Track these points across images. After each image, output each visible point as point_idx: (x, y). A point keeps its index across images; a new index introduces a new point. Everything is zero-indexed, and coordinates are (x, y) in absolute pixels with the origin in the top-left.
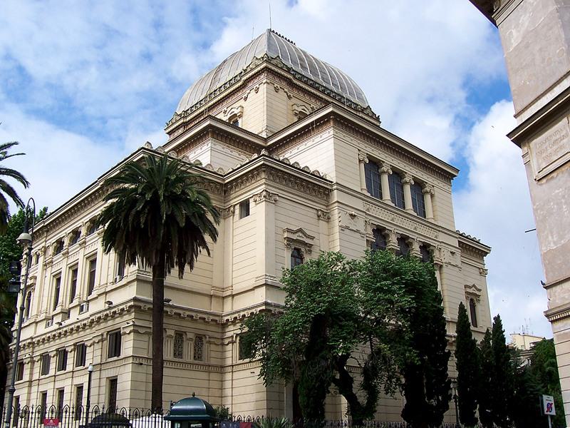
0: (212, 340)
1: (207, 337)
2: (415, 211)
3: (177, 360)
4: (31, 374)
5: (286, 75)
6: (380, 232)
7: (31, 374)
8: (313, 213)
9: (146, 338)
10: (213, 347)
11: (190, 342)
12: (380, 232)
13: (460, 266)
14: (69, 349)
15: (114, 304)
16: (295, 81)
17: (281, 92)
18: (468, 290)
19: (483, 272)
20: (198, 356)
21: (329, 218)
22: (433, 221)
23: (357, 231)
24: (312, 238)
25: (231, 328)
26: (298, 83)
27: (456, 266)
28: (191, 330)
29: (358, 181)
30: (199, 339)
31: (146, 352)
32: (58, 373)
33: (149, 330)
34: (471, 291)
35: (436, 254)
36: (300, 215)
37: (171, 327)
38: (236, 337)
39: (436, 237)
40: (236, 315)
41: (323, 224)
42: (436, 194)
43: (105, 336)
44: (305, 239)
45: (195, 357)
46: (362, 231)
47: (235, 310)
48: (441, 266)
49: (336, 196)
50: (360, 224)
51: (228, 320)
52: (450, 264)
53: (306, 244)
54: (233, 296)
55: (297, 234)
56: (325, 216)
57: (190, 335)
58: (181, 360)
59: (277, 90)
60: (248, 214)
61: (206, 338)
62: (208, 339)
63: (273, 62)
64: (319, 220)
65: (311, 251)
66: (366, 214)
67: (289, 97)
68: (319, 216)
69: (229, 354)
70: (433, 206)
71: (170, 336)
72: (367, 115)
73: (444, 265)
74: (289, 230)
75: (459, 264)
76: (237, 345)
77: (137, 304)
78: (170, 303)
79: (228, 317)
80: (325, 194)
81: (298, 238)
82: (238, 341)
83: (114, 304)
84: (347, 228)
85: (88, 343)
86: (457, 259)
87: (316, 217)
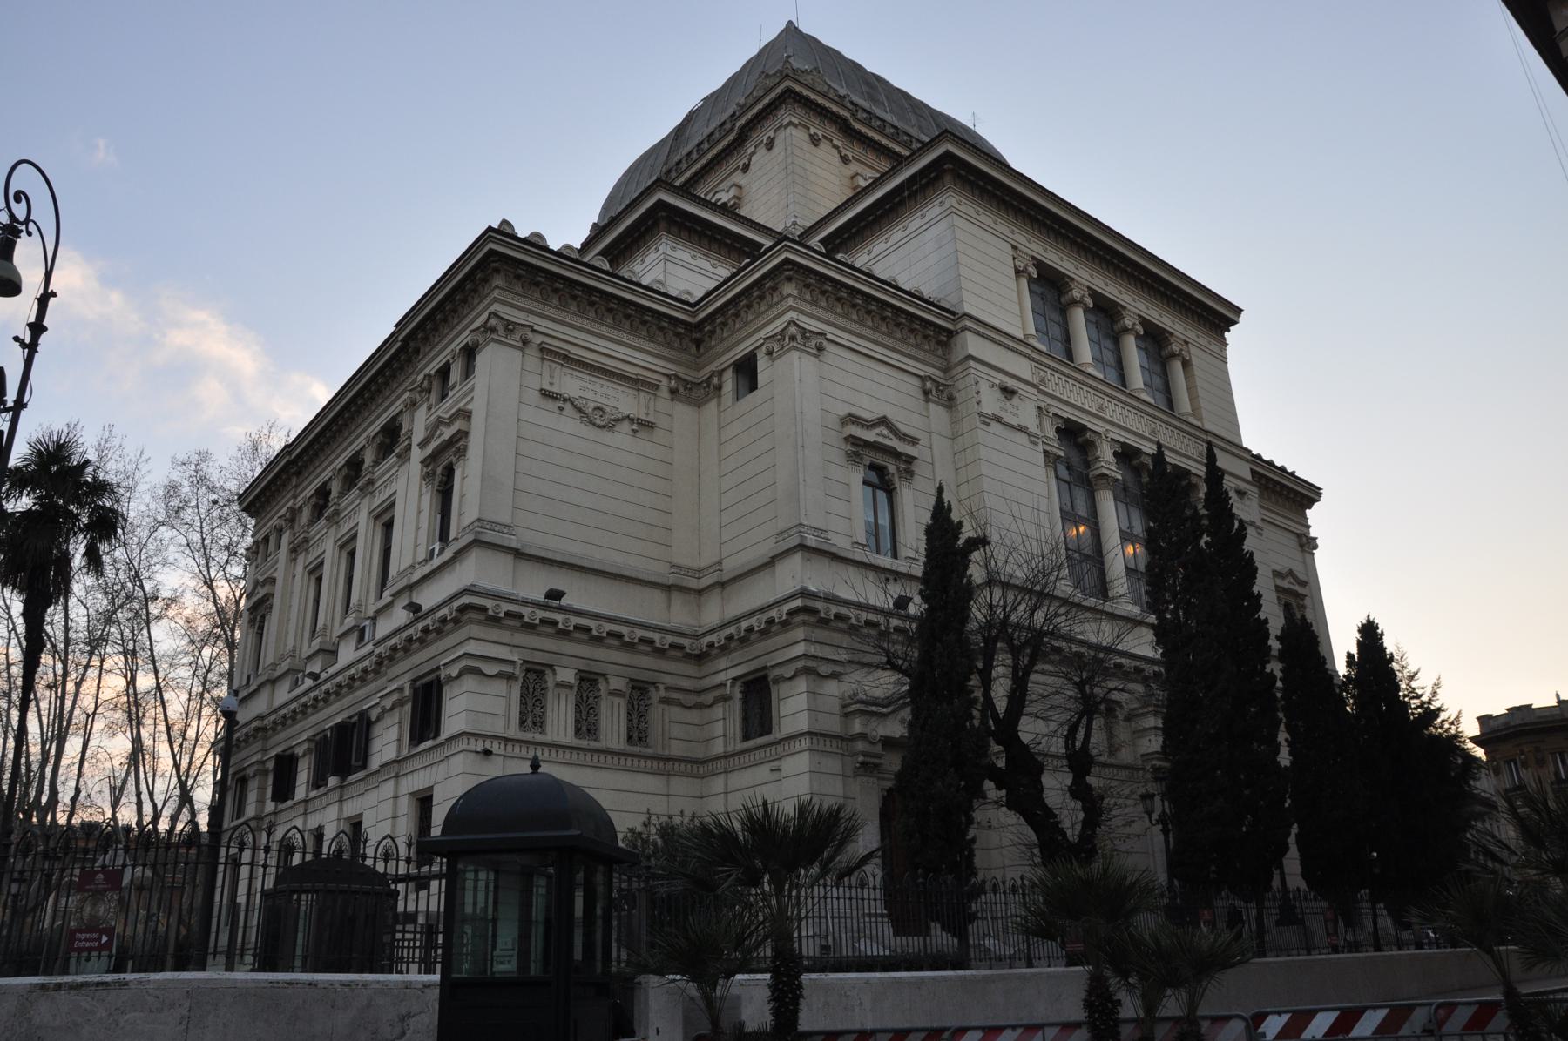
0: (674, 695)
1: (661, 687)
3: (584, 743)
6: (1072, 433)
9: (500, 687)
10: (675, 712)
11: (617, 700)
13: (1259, 523)
15: (425, 608)
18: (1279, 582)
20: (637, 734)
21: (951, 398)
22: (1192, 420)
25: (722, 663)
28: (617, 666)
30: (639, 689)
31: (501, 722)
33: (508, 669)
34: (1285, 584)
37: (565, 660)
38: (733, 685)
40: (731, 630)
46: (1033, 428)
49: (973, 345)
50: (1025, 412)
51: (711, 645)
54: (722, 585)
55: (877, 431)
57: (617, 683)
58: (593, 745)
60: (753, 386)
61: (657, 689)
62: (662, 693)
64: (927, 401)
66: (1040, 391)
68: (926, 393)
71: (562, 685)
76: (737, 705)
78: (564, 602)
79: (713, 638)
80: (939, 343)
81: (880, 440)
82: (738, 695)
83: (425, 608)
87: (921, 397)
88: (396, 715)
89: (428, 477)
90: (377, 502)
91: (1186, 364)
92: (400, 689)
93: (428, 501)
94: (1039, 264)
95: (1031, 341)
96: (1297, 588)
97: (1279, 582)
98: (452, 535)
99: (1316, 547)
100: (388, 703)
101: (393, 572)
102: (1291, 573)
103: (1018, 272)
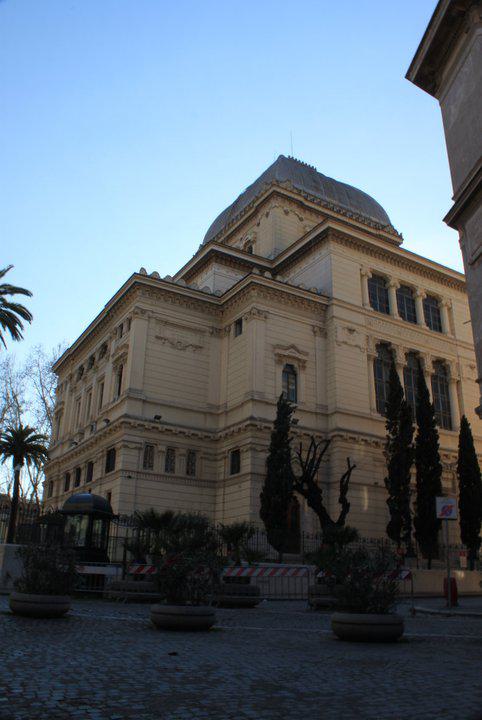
4: (58, 491)
5: (296, 197)
7: (58, 491)
12: (385, 347)
14: (82, 467)
16: (307, 203)
17: (291, 214)
21: (326, 333)
24: (307, 354)
26: (311, 205)
41: (319, 339)
44: (297, 355)
47: (229, 424)
53: (299, 360)
56: (323, 332)
59: (286, 213)
60: (241, 333)
63: (283, 185)
65: (304, 367)
67: (301, 220)
68: (315, 332)
72: (388, 233)
77: (126, 420)
84: (346, 343)
85: (94, 460)
89: (114, 369)
93: (115, 378)
101: (103, 404)
103: (362, 276)
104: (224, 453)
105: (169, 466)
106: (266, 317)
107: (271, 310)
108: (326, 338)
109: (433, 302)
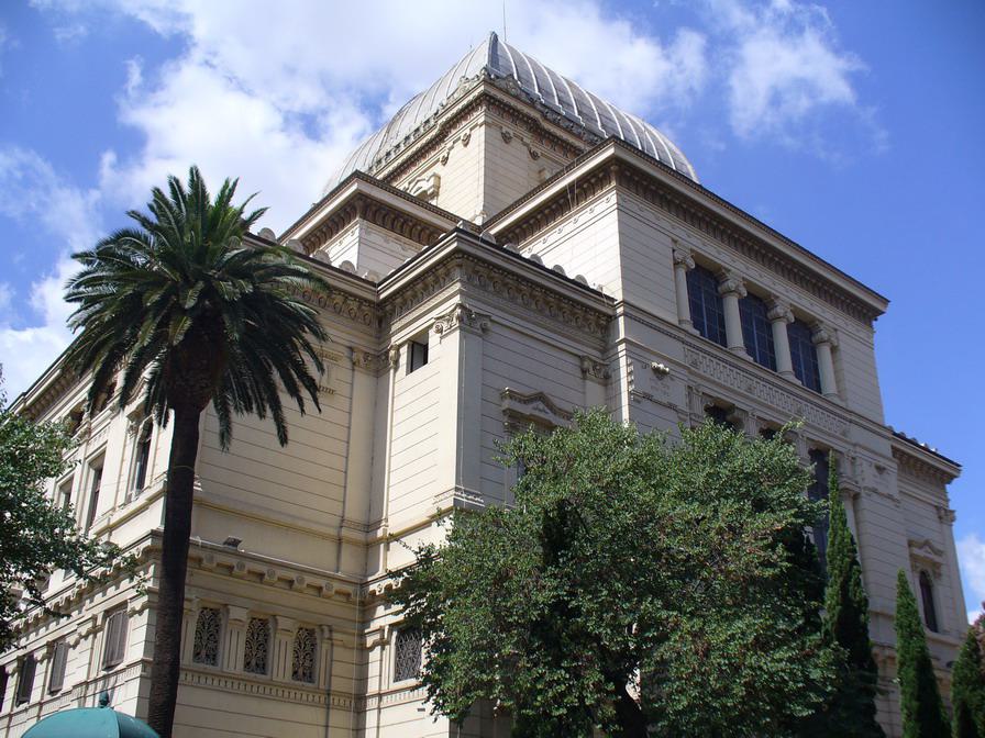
2: (798, 376)
8: (571, 365)
13: (897, 496)
14: (38, 656)
18: (916, 551)
19: (945, 516)
21: (607, 377)
22: (836, 400)
23: (671, 406)
27: (890, 497)
29: (672, 304)
32: (16, 710)
34: (921, 553)
35: (846, 468)
36: (545, 365)
39: (844, 434)
42: (842, 346)
43: (99, 622)
45: (295, 673)
48: (856, 497)
50: (677, 393)
52: (875, 491)
55: (535, 404)
64: (584, 378)
66: (691, 373)
68: (584, 372)
69: (373, 670)
70: (836, 372)
73: (863, 493)
74: (512, 395)
75: (894, 492)
81: (537, 413)
84: (648, 397)
86: (892, 483)
88: (85, 644)
89: (133, 429)
90: (92, 448)
91: (834, 350)
92: (94, 618)
93: (131, 450)
94: (697, 257)
95: (685, 326)
96: (933, 556)
97: (916, 551)
98: (147, 484)
99: (953, 520)
100: (83, 630)
101: (99, 513)
102: (927, 543)
103: (676, 264)
104: (381, 630)
105: (257, 662)
106: (485, 330)
107: (497, 315)
108: (606, 385)
109: (804, 331)
